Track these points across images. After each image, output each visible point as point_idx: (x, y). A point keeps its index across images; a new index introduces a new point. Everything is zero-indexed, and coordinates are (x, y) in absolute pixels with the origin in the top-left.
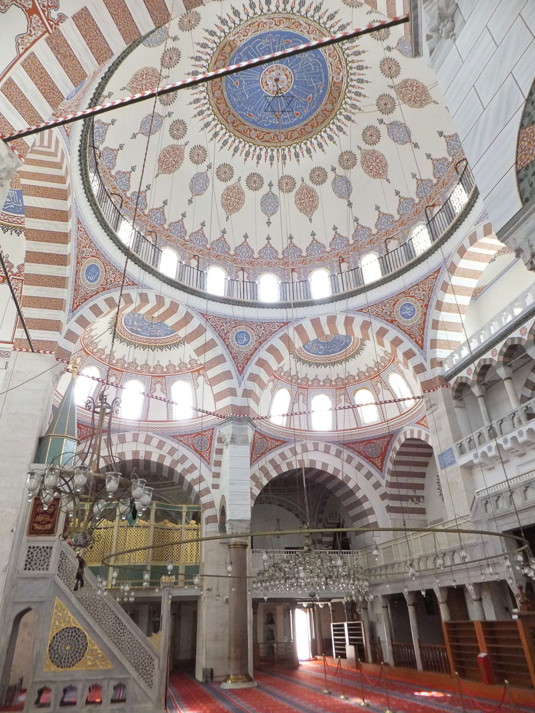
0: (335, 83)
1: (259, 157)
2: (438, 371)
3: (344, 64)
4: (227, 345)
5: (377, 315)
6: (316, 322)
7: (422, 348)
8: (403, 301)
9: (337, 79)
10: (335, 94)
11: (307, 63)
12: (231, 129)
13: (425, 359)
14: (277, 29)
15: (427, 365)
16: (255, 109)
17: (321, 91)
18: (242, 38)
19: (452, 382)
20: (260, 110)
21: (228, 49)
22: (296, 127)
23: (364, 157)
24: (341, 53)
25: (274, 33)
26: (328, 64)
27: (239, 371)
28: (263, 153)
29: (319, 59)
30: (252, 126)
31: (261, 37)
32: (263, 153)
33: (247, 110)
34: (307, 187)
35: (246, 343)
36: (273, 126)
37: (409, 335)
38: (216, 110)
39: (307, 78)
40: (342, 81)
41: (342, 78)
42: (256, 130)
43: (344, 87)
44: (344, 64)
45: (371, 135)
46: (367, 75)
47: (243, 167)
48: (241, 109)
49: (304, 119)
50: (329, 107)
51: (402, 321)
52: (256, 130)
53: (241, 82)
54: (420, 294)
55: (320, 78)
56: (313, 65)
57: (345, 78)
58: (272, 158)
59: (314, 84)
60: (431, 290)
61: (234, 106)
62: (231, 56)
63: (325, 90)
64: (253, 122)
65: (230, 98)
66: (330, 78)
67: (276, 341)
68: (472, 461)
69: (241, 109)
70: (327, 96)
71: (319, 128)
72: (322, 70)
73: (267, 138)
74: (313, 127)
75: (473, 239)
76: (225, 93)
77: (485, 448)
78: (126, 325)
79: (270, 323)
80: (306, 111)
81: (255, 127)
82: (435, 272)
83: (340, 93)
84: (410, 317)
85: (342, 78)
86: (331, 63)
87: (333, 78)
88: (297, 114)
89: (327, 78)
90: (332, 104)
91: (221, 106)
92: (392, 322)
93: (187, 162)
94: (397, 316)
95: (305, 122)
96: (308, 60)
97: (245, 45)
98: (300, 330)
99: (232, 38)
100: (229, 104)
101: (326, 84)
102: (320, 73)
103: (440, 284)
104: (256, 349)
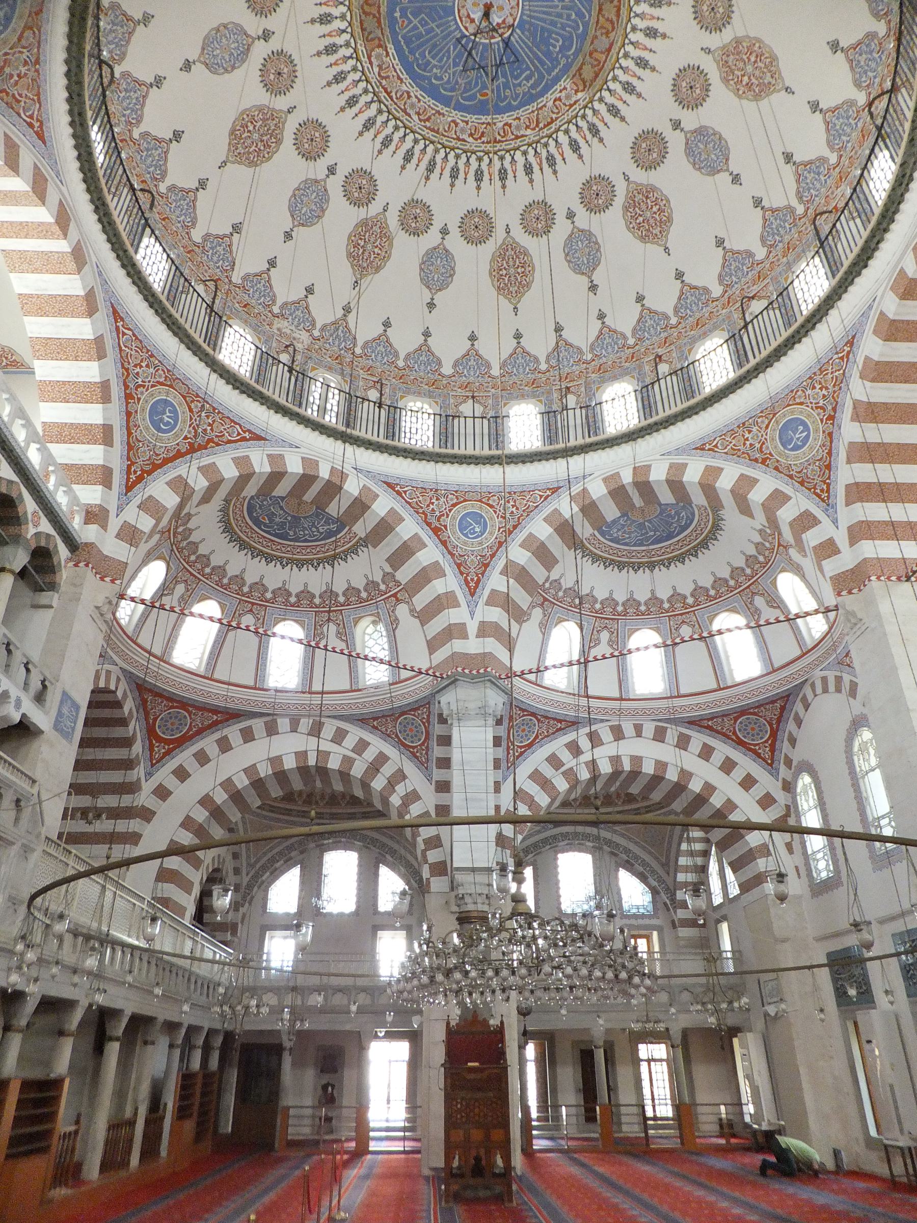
0: (380, 46)
9: (378, 56)
10: (370, 23)
11: (440, 60)
17: (397, 15)
18: (563, 94)
24: (392, 107)
25: (510, 108)
26: (404, 76)
29: (424, 78)
31: (530, 98)
39: (432, 30)
40: (369, 57)
41: (371, 63)
43: (361, 48)
55: (408, 42)
56: (428, 63)
59: (415, 22)
62: (580, 58)
63: (392, 27)
66: (391, 48)
70: (384, 9)
72: (411, 58)
82: (41, 126)
83: (363, 30)
85: (371, 63)
86: (401, 80)
87: (388, 54)
89: (399, 50)
96: (441, 68)
97: (557, 80)
99: (580, 95)
101: (394, 33)
102: (412, 52)
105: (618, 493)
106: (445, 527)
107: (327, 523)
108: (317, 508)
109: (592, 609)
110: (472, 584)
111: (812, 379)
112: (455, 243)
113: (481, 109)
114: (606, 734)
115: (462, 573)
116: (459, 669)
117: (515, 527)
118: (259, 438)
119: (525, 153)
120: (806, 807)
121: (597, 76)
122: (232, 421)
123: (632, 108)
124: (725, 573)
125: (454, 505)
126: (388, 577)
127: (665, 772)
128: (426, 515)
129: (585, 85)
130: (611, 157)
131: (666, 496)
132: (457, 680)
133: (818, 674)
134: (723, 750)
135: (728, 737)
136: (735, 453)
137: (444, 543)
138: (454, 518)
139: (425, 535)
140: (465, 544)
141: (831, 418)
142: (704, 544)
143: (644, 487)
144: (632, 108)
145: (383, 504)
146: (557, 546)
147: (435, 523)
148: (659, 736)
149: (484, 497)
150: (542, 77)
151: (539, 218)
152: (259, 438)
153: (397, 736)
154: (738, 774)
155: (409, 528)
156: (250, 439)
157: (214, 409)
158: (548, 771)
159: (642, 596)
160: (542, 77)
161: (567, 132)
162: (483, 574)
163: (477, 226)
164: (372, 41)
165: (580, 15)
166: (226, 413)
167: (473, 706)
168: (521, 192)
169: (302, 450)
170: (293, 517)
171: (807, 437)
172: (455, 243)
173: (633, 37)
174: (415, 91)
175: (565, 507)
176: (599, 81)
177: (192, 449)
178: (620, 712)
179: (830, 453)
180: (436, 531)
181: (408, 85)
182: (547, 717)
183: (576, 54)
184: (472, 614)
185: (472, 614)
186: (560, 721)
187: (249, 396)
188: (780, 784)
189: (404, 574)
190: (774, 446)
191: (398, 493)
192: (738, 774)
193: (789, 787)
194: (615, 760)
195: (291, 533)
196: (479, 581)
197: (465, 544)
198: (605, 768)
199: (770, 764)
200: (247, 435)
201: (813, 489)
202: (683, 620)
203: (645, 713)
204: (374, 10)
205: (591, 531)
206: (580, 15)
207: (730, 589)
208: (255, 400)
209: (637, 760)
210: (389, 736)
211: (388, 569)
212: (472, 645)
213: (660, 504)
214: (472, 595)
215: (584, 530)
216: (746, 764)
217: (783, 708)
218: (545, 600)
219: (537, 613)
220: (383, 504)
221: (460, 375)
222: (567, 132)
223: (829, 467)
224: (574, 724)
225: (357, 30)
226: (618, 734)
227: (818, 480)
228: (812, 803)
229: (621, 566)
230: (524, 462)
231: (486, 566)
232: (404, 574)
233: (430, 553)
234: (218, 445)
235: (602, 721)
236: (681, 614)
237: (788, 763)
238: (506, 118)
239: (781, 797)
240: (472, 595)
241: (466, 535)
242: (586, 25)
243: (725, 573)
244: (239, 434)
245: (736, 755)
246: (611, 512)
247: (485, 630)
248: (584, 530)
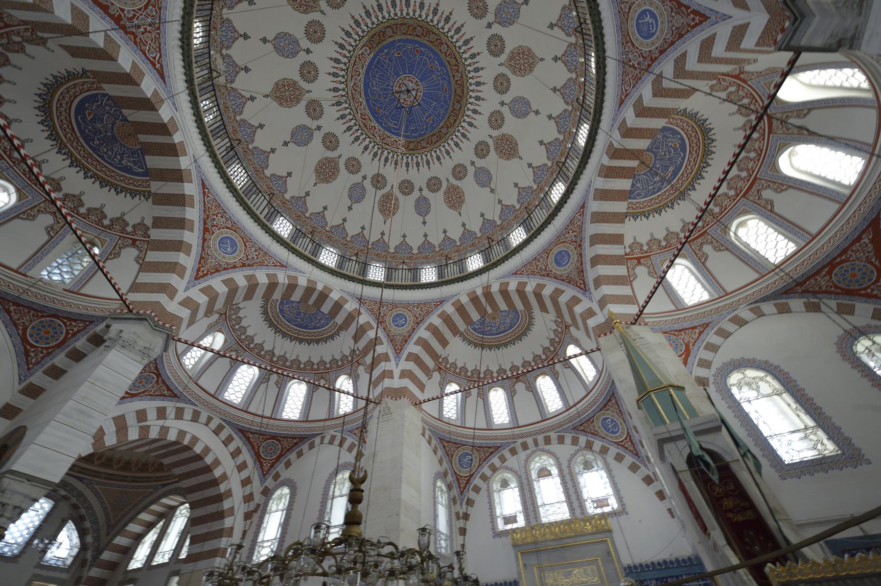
3: (353, 59)
9: (366, 50)
10: (376, 39)
12: (464, 100)
16: (439, 89)
20: (437, 85)
22: (426, 42)
24: (350, 70)
25: (380, 124)
27: (701, 22)
30: (453, 83)
33: (445, 97)
36: (442, 64)
38: (457, 123)
40: (364, 46)
42: (454, 76)
43: (365, 39)
44: (353, 59)
46: (339, 36)
48: (446, 102)
50: (389, 32)
52: (454, 76)
53: (427, 118)
55: (378, 62)
57: (360, 46)
58: (466, 42)
61: (447, 109)
64: (449, 84)
65: (443, 118)
66: (371, 56)
69: (446, 102)
70: (385, 43)
71: (410, 22)
73: (453, 62)
74: (415, 29)
76: (441, 125)
80: (409, 46)
81: (452, 79)
88: (417, 51)
90: (384, 32)
91: (452, 121)
95: (417, 38)
105: (310, 290)
106: (213, 233)
107: (135, 163)
108: (141, 149)
109: (239, 337)
111: (419, 305)
112: (318, 137)
113: (373, 112)
114: (188, 415)
115: (200, 263)
116: (153, 314)
117: (249, 265)
118: (163, 77)
119: (370, 142)
120: (274, 508)
121: (413, 150)
122: (159, 48)
123: (413, 170)
124: (315, 360)
125: (227, 228)
126: (141, 226)
127: (206, 455)
128: (208, 218)
129: (407, 148)
130: (394, 176)
131: (326, 308)
132: (145, 319)
133: (332, 432)
134: (246, 456)
135: (253, 448)
136: (371, 311)
137: (204, 240)
138: (222, 233)
139: (198, 226)
140: (216, 250)
141: (418, 323)
142: (317, 342)
143: (323, 296)
144: (413, 170)
145: (190, 189)
146: (260, 292)
147: (209, 226)
148: (217, 431)
149: (247, 239)
152: (163, 77)
153: (25, 330)
154: (245, 474)
155: (193, 214)
156: (157, 70)
157: (159, 28)
158: (131, 420)
159: (267, 347)
161: (389, 153)
162: (212, 273)
163: (331, 142)
164: (370, 44)
166: (162, 40)
167: (141, 344)
168: (356, 151)
169: (178, 114)
170: (114, 137)
171: (404, 325)
172: (318, 137)
173: (433, 153)
174: (362, 76)
175: (282, 278)
176: (411, 152)
178: (206, 404)
179: (409, 336)
181: (362, 72)
182: (164, 382)
183: (414, 137)
184: (187, 289)
185: (187, 289)
186: (169, 389)
187: (183, 54)
188: (261, 489)
189: (156, 234)
190: (389, 319)
191: (204, 193)
192: (245, 474)
193: (267, 493)
194: (182, 433)
195: (96, 142)
196: (206, 275)
197: (216, 250)
198: (172, 436)
199: (264, 475)
200: (158, 66)
201: (394, 346)
202: (275, 372)
203: (220, 412)
204: (382, 38)
207: (312, 369)
208: (184, 61)
209: (195, 439)
210: (16, 325)
211: (149, 222)
212: (173, 307)
213: (318, 310)
214: (196, 279)
215: (277, 295)
216: (252, 470)
217: (296, 444)
218: (225, 314)
219: (215, 317)
220: (190, 189)
221: (271, 181)
222: (389, 153)
223: (406, 341)
224: (174, 395)
225: (371, 34)
226: (195, 417)
227: (398, 344)
228: (281, 506)
229: (271, 325)
230: (278, 242)
231: (217, 271)
232: (156, 234)
233: (192, 237)
234: (135, 43)
235: (193, 404)
237: (276, 477)
238: (377, 125)
239: (258, 498)
240: (196, 279)
241: (220, 247)
243: (315, 360)
244: (154, 58)
245: (250, 462)
246: (296, 296)
247: (187, 303)
248: (277, 295)
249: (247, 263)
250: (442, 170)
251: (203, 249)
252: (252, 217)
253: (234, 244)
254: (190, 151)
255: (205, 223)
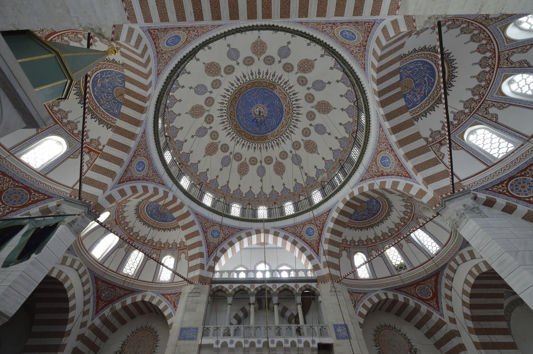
1: (222, 116)
2: (210, 275)
4: (131, 160)
5: (201, 223)
6: (175, 199)
7: (209, 256)
8: (217, 228)
12: (232, 98)
13: (207, 264)
14: (284, 106)
15: (206, 268)
19: (214, 286)
21: (272, 87)
23: (243, 163)
28: (225, 117)
30: (235, 107)
32: (225, 117)
34: (217, 146)
35: (139, 171)
37: (208, 245)
45: (253, 161)
47: (215, 110)
49: (246, 130)
51: (209, 236)
53: (256, 96)
54: (226, 231)
58: (223, 123)
60: (232, 234)
61: (243, 96)
65: (247, 93)
67: (151, 186)
68: (213, 344)
73: (232, 116)
75: (267, 232)
77: (228, 340)
78: (102, 72)
79: (158, 175)
84: (218, 238)
91: (243, 90)
92: (205, 232)
93: (212, 79)
94: (209, 231)
98: (166, 195)
100: (244, 93)
103: (238, 235)
104: (139, 179)
110: (407, 175)
115: (401, 176)
117: (391, 147)
118: (330, 210)
129: (275, 87)
130: (292, 78)
137: (388, 175)
138: (380, 166)
150: (274, 98)
151: (310, 98)
152: (330, 210)
160: (274, 98)
165: (259, 91)
173: (261, 77)
175: (387, 125)
177: (322, 230)
180: (382, 175)
191: (365, 179)
196: (406, 171)
205: (408, 113)
206: (259, 91)
231: (402, 165)
236: (499, 59)
240: (411, 178)
241: (388, 166)
242: (261, 89)
249: (390, 149)
250: (259, 66)
251: (393, 175)
252: (365, 151)
253: (383, 158)
254: (350, 191)
255: (379, 176)
